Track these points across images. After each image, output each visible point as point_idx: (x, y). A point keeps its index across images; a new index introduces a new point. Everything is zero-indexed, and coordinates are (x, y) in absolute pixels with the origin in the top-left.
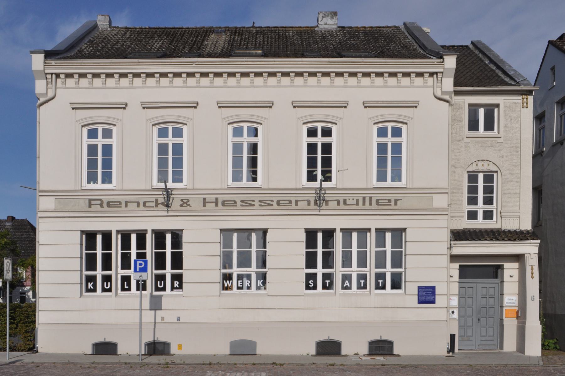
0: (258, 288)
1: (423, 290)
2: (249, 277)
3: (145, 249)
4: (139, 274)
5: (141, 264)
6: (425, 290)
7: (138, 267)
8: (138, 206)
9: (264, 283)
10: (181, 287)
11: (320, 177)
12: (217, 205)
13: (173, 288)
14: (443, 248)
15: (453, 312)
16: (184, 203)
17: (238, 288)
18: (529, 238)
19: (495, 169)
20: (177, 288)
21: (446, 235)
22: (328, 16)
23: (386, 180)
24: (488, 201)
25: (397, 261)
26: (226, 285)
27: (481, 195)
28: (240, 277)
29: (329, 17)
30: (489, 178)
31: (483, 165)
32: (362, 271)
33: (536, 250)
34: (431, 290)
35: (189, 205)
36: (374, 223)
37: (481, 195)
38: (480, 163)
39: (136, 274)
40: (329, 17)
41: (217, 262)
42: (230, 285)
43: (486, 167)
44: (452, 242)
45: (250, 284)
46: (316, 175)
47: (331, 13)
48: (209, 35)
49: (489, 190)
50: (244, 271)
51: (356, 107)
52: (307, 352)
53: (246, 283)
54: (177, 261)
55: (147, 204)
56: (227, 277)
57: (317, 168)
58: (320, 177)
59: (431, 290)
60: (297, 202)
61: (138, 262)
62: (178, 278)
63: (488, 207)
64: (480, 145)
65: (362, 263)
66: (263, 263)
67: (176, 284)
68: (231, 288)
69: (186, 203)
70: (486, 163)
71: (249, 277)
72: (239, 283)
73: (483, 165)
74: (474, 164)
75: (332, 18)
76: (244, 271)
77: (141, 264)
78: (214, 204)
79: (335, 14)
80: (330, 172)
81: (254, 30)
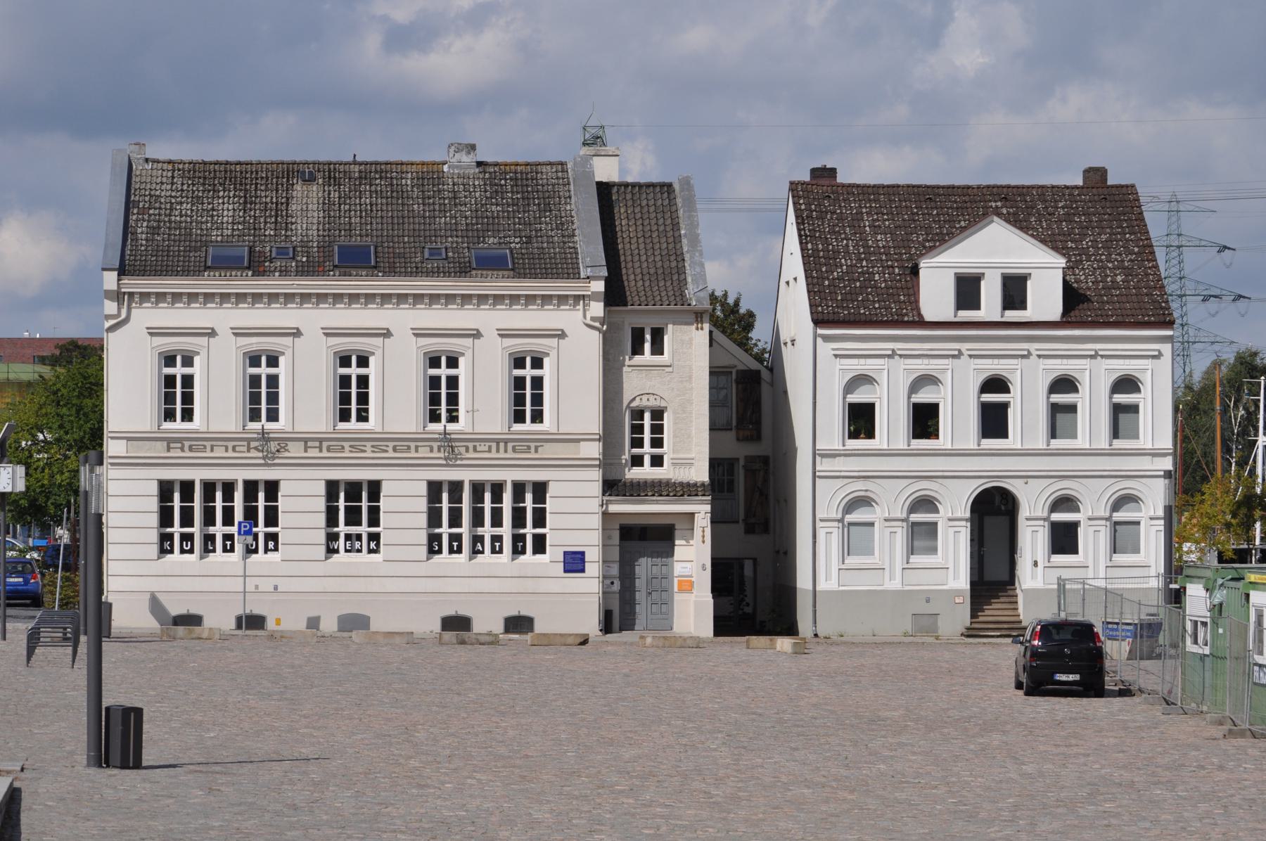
0: (370, 551)
1: (569, 556)
2: (359, 537)
3: (233, 502)
4: (244, 537)
5: (245, 527)
6: (573, 556)
7: (243, 529)
8: (227, 451)
9: (378, 545)
10: (276, 549)
11: (444, 415)
12: (321, 451)
13: (266, 550)
14: (594, 505)
15: (612, 583)
16: (282, 447)
17: (347, 551)
18: (700, 493)
19: (663, 404)
20: (271, 550)
21: (597, 488)
22: (462, 151)
23: (524, 421)
24: (657, 443)
25: (540, 520)
26: (331, 547)
27: (647, 436)
28: (348, 537)
29: (464, 152)
30: (658, 414)
31: (648, 400)
32: (497, 531)
33: (708, 508)
34: (580, 556)
35: (287, 450)
36: (509, 476)
37: (647, 436)
38: (645, 398)
39: (241, 537)
40: (464, 152)
41: (321, 519)
42: (336, 547)
43: (653, 403)
44: (605, 498)
45: (361, 546)
46: (440, 414)
47: (467, 146)
48: (293, 184)
49: (657, 429)
50: (353, 530)
51: (490, 336)
52: (431, 629)
53: (357, 545)
54: (272, 519)
55: (237, 449)
56: (332, 537)
57: (440, 405)
58: (444, 415)
59: (580, 556)
60: (417, 447)
61: (243, 524)
62: (273, 537)
63: (657, 451)
64: (644, 375)
65: (497, 522)
66: (374, 521)
67: (271, 545)
68: (337, 551)
69: (284, 448)
70: (652, 398)
71: (359, 537)
72: (348, 545)
73: (648, 400)
74: (638, 399)
75: (469, 153)
76: (353, 530)
77: (245, 527)
78: (318, 449)
79: (472, 148)
80: (457, 410)
81: (357, 168)
